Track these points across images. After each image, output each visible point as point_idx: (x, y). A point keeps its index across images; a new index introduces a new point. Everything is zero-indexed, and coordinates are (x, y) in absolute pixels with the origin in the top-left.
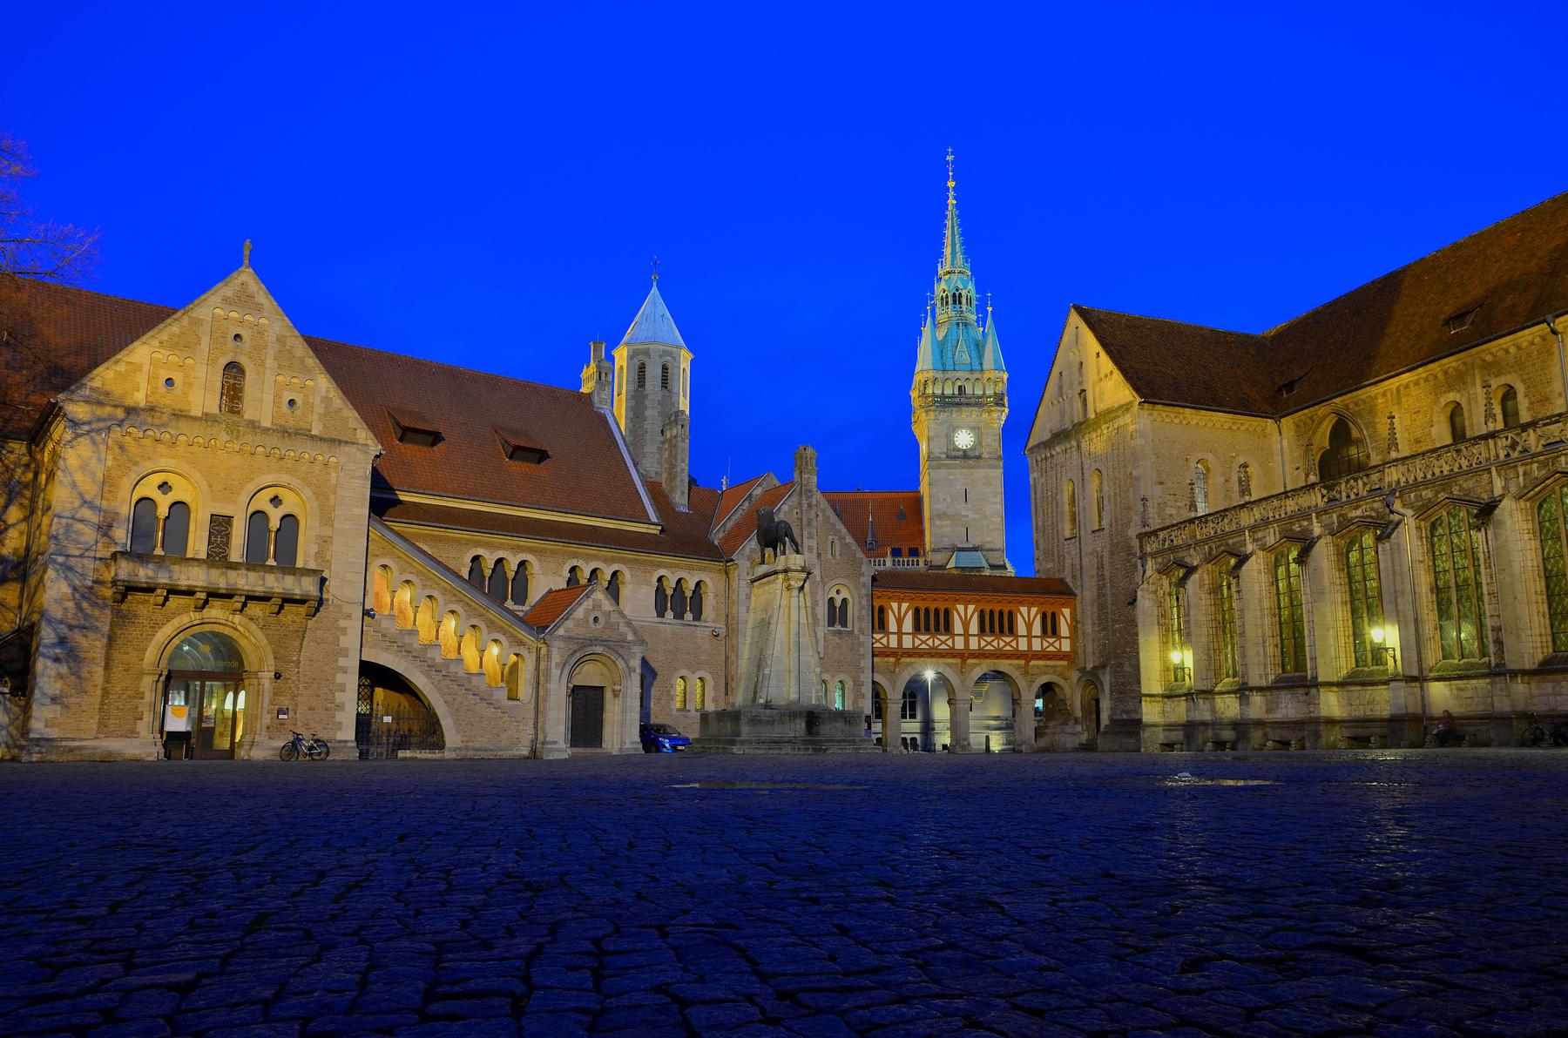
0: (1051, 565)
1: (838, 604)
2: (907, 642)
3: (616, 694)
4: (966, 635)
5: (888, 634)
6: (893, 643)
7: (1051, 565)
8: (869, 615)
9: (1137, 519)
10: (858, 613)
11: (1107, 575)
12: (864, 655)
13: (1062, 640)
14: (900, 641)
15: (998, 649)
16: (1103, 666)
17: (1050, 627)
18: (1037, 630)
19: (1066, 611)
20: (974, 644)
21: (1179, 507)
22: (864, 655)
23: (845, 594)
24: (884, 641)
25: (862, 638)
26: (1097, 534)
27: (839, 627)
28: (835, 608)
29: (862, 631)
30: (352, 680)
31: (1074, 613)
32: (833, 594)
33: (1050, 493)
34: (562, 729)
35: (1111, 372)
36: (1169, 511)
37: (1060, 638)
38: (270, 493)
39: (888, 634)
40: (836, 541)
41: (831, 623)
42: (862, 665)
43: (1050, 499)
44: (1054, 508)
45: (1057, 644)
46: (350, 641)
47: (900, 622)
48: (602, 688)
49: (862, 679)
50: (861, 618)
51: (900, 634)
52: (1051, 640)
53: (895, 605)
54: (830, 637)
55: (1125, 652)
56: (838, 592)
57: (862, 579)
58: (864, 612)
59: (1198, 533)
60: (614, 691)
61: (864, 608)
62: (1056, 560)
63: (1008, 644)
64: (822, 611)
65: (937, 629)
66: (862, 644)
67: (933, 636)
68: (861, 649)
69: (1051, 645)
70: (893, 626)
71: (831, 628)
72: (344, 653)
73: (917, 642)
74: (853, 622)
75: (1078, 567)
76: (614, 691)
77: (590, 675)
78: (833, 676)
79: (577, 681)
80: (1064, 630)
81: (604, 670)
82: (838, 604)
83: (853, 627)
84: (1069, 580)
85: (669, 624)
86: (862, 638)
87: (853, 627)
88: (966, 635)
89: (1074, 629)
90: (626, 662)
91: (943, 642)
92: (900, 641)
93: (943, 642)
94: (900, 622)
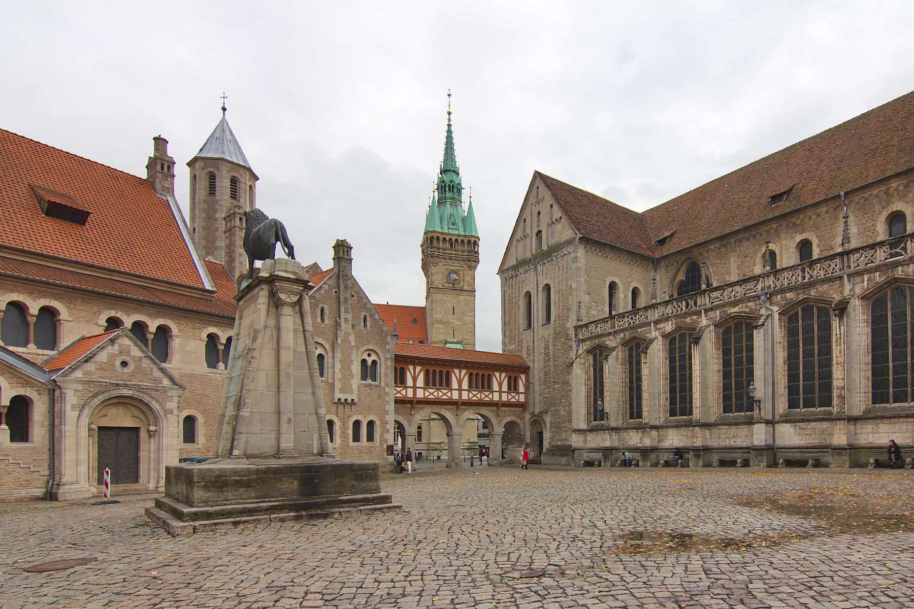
0: (514, 346)
1: (369, 363)
2: (420, 394)
3: (150, 434)
4: (460, 390)
6: (410, 394)
7: (514, 346)
8: (392, 373)
9: (573, 316)
10: (386, 369)
11: (551, 354)
12: (388, 402)
13: (520, 395)
14: (415, 393)
15: (480, 400)
16: (546, 412)
17: (513, 387)
18: (505, 388)
19: (523, 376)
20: (465, 396)
21: (599, 311)
22: (388, 402)
24: (404, 392)
25: (387, 389)
26: (545, 326)
27: (369, 381)
28: (367, 367)
29: (387, 385)
31: (527, 378)
32: (365, 357)
33: (514, 300)
34: (83, 469)
35: (561, 218)
36: (594, 312)
37: (519, 393)
39: (406, 388)
40: (368, 318)
41: (364, 377)
42: (387, 409)
43: (514, 304)
44: (517, 310)
45: (517, 397)
47: (415, 379)
49: (386, 419)
50: (386, 375)
51: (415, 388)
52: (513, 395)
53: (411, 368)
54: (362, 388)
55: (562, 402)
56: (369, 355)
57: (388, 347)
58: (389, 371)
59: (616, 325)
60: (149, 431)
61: (389, 368)
62: (517, 344)
63: (487, 396)
64: (356, 368)
65: (441, 385)
66: (387, 394)
67: (438, 390)
68: (387, 398)
69: (513, 398)
70: (410, 382)
71: (363, 382)
73: (427, 394)
74: (380, 378)
75: (531, 348)
76: (149, 431)
77: (122, 419)
78: (365, 417)
79: (105, 422)
80: (521, 389)
81: (137, 413)
82: (369, 363)
83: (380, 381)
84: (525, 356)
85: (220, 374)
86: (387, 389)
87: (380, 381)
88: (460, 390)
89: (527, 387)
90: (160, 405)
91: (445, 394)
92: (415, 393)
93: (445, 394)
94: (415, 379)
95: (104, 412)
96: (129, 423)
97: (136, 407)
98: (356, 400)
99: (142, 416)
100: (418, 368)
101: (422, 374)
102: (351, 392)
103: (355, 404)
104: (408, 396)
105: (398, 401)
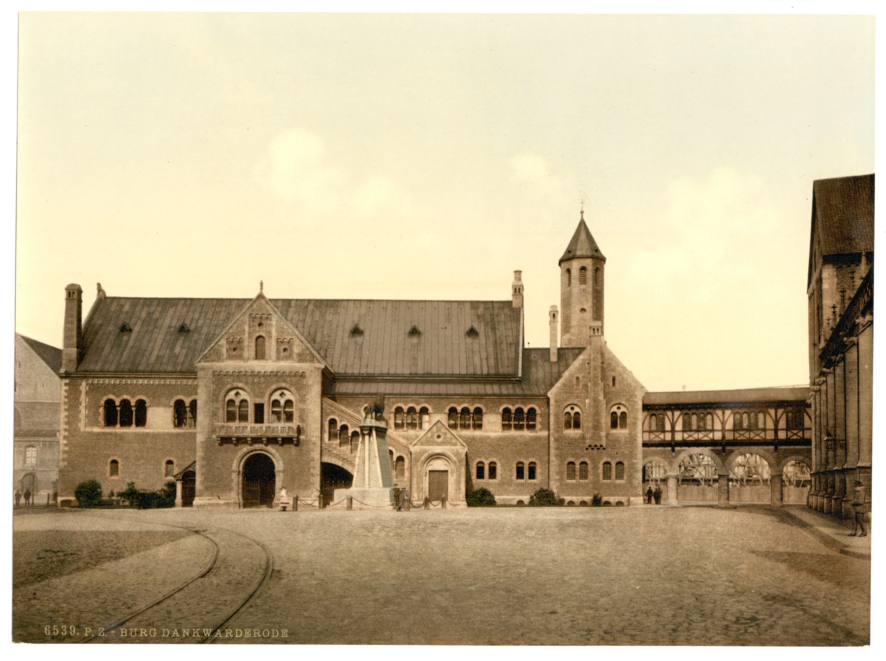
1: (619, 414)
2: (679, 437)
5: (664, 431)
6: (668, 437)
23: (623, 409)
30: (317, 471)
38: (279, 392)
39: (664, 431)
46: (316, 455)
48: (447, 471)
51: (673, 431)
53: (669, 413)
70: (668, 427)
72: (313, 460)
79: (431, 468)
81: (446, 462)
82: (619, 414)
95: (431, 462)
96: (443, 468)
97: (446, 460)
98: (604, 445)
99: (448, 464)
100: (677, 413)
101: (680, 421)
102: (600, 438)
103: (604, 449)
104: (666, 439)
105: (645, 445)
